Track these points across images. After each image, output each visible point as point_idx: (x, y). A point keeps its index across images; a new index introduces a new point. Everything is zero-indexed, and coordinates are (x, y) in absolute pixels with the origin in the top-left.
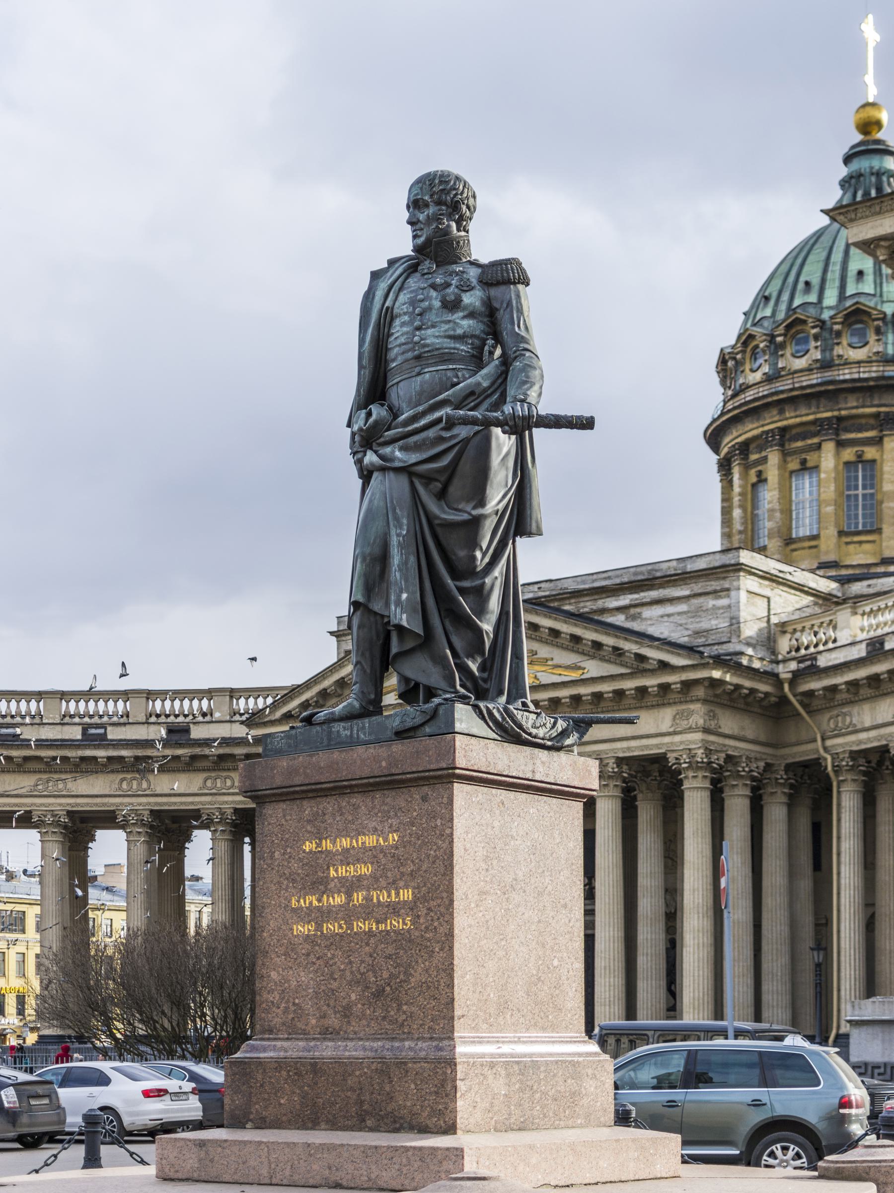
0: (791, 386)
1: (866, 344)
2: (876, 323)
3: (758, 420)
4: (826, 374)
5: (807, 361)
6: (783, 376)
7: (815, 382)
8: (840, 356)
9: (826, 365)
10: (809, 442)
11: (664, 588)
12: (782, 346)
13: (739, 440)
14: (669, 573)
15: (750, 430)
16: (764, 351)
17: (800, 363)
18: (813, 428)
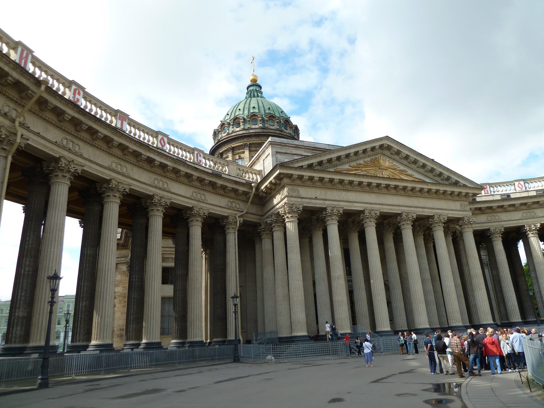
16: (260, 120)
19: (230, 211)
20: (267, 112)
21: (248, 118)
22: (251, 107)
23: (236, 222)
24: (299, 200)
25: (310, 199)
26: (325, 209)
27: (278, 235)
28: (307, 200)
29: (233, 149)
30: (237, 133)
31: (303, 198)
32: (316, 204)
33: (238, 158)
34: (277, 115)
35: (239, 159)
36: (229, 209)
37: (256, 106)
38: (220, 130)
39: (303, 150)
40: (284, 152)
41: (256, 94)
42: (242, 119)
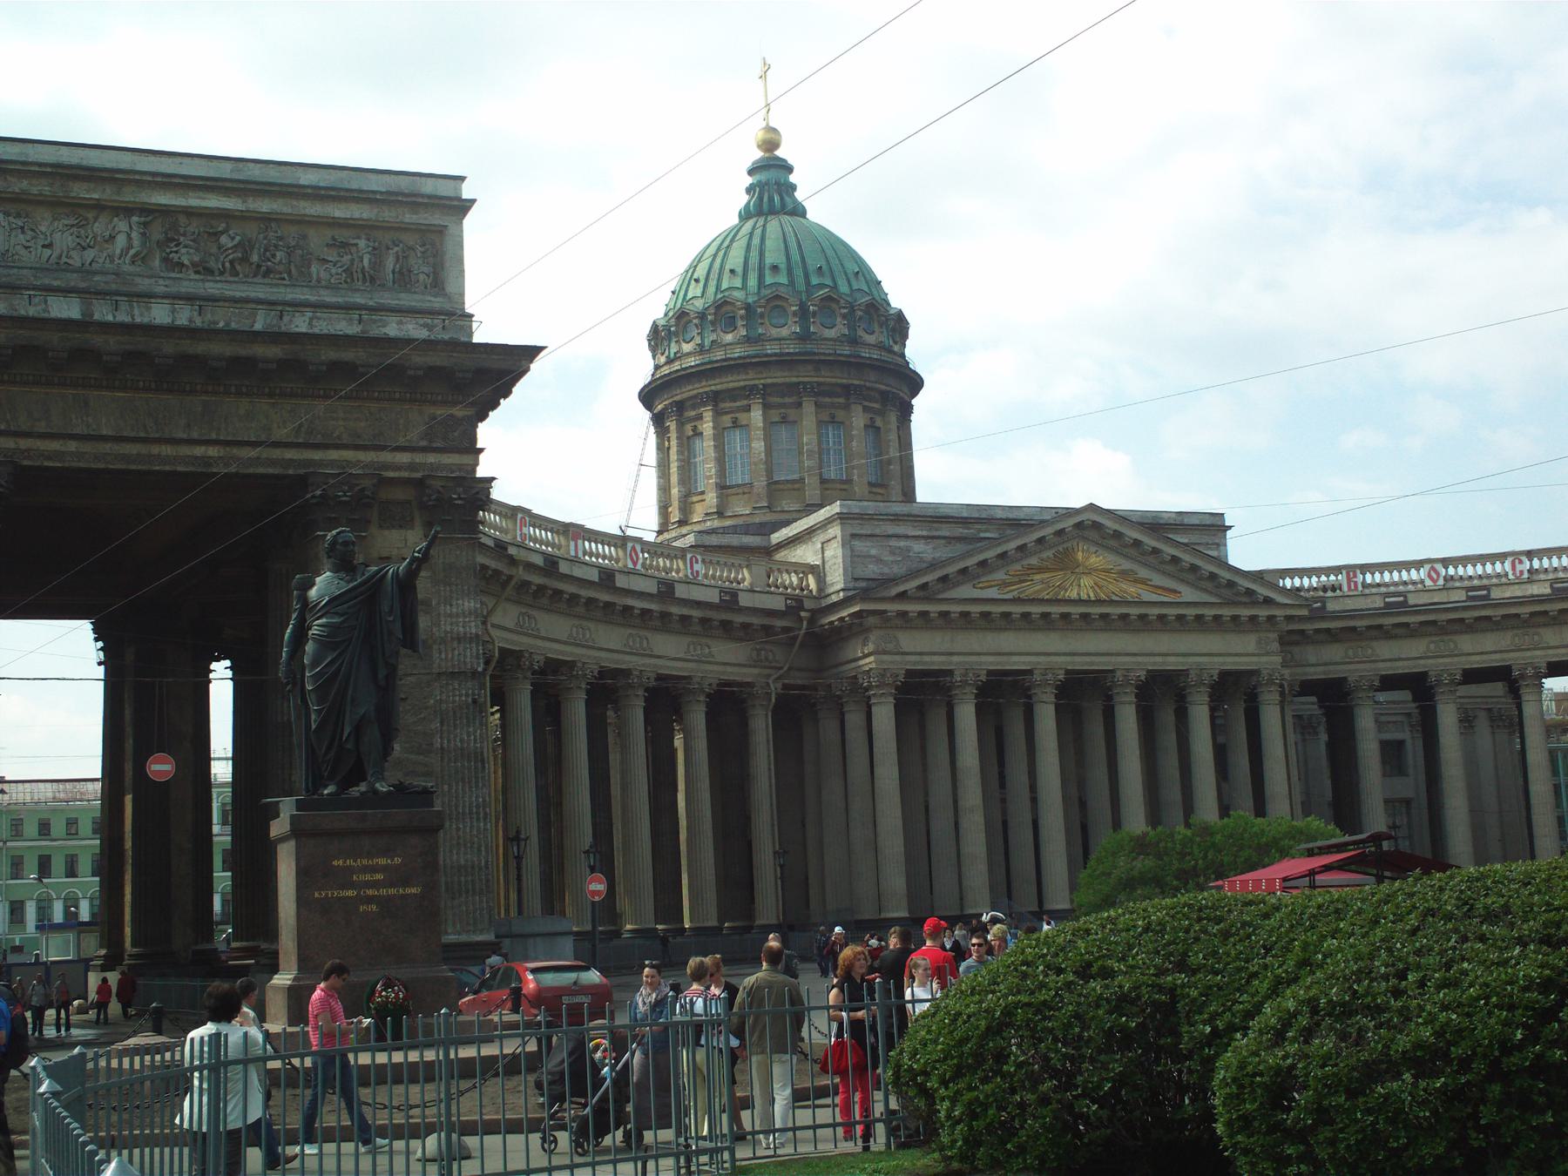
10: (837, 400)
13: (762, 381)
15: (779, 377)
16: (795, 314)
19: (756, 671)
20: (815, 281)
21: (760, 307)
22: (767, 267)
23: (771, 694)
24: (898, 658)
25: (921, 654)
26: (950, 673)
27: (854, 719)
28: (913, 658)
29: (715, 398)
31: (907, 654)
32: (933, 663)
34: (844, 288)
36: (755, 667)
37: (781, 261)
38: (672, 329)
40: (869, 532)
41: (776, 198)
42: (742, 309)
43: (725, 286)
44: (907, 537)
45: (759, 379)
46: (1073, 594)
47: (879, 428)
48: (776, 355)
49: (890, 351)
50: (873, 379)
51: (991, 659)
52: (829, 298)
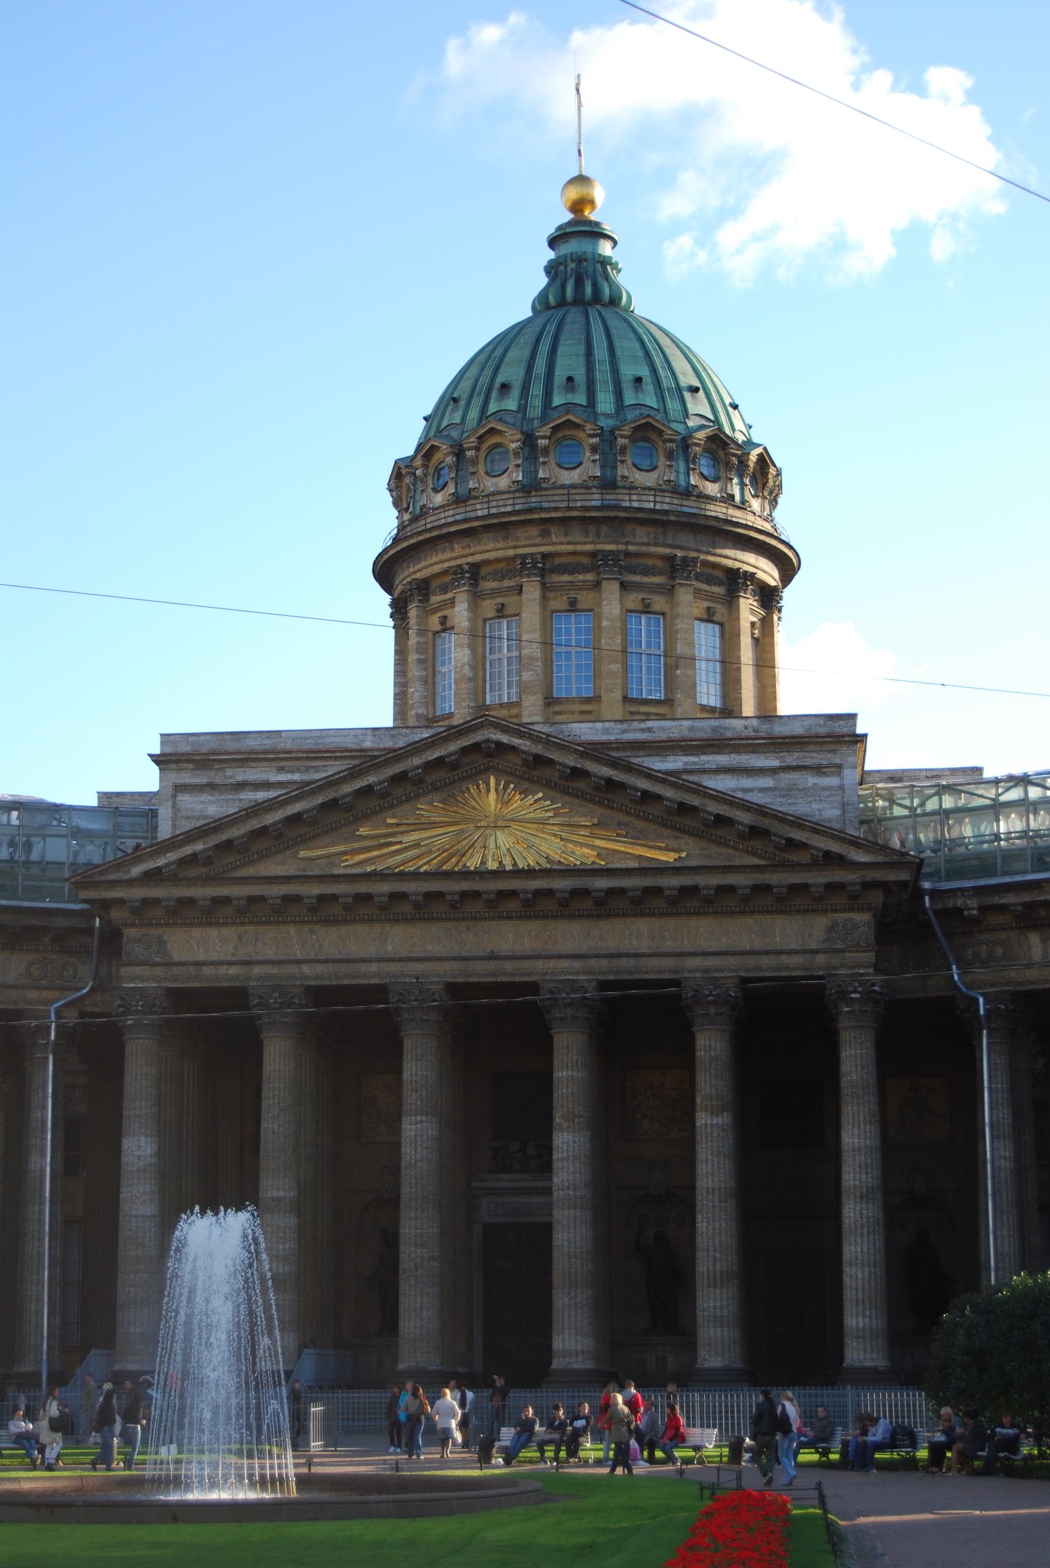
0: (565, 504)
1: (654, 468)
2: (668, 445)
3: (506, 538)
4: (608, 497)
5: (580, 476)
6: (546, 489)
7: (593, 503)
8: (623, 477)
9: (608, 484)
10: (581, 577)
11: (739, 753)
12: (545, 451)
13: (470, 559)
14: (744, 735)
16: (516, 454)
17: (568, 477)
18: (585, 561)
19: (32, 994)
21: (469, 449)
24: (159, 971)
25: (198, 964)
29: (423, 588)
30: (430, 521)
31: (176, 964)
33: (439, 628)
34: (605, 403)
35: (444, 630)
39: (274, 764)
40: (205, 781)
43: (444, 424)
44: (266, 785)
45: (466, 556)
46: (473, 863)
47: (663, 614)
48: (477, 518)
49: (688, 492)
50: (646, 540)
51: (319, 968)
52: (569, 424)
